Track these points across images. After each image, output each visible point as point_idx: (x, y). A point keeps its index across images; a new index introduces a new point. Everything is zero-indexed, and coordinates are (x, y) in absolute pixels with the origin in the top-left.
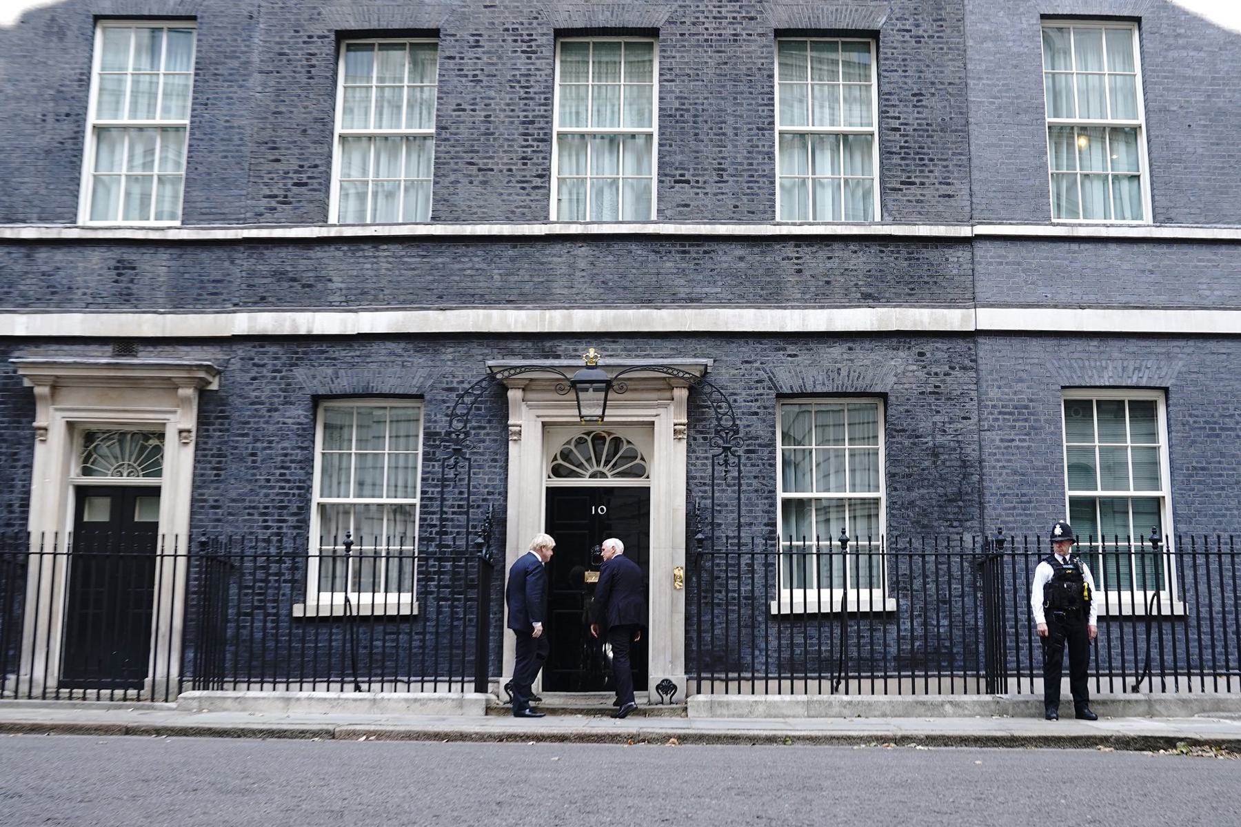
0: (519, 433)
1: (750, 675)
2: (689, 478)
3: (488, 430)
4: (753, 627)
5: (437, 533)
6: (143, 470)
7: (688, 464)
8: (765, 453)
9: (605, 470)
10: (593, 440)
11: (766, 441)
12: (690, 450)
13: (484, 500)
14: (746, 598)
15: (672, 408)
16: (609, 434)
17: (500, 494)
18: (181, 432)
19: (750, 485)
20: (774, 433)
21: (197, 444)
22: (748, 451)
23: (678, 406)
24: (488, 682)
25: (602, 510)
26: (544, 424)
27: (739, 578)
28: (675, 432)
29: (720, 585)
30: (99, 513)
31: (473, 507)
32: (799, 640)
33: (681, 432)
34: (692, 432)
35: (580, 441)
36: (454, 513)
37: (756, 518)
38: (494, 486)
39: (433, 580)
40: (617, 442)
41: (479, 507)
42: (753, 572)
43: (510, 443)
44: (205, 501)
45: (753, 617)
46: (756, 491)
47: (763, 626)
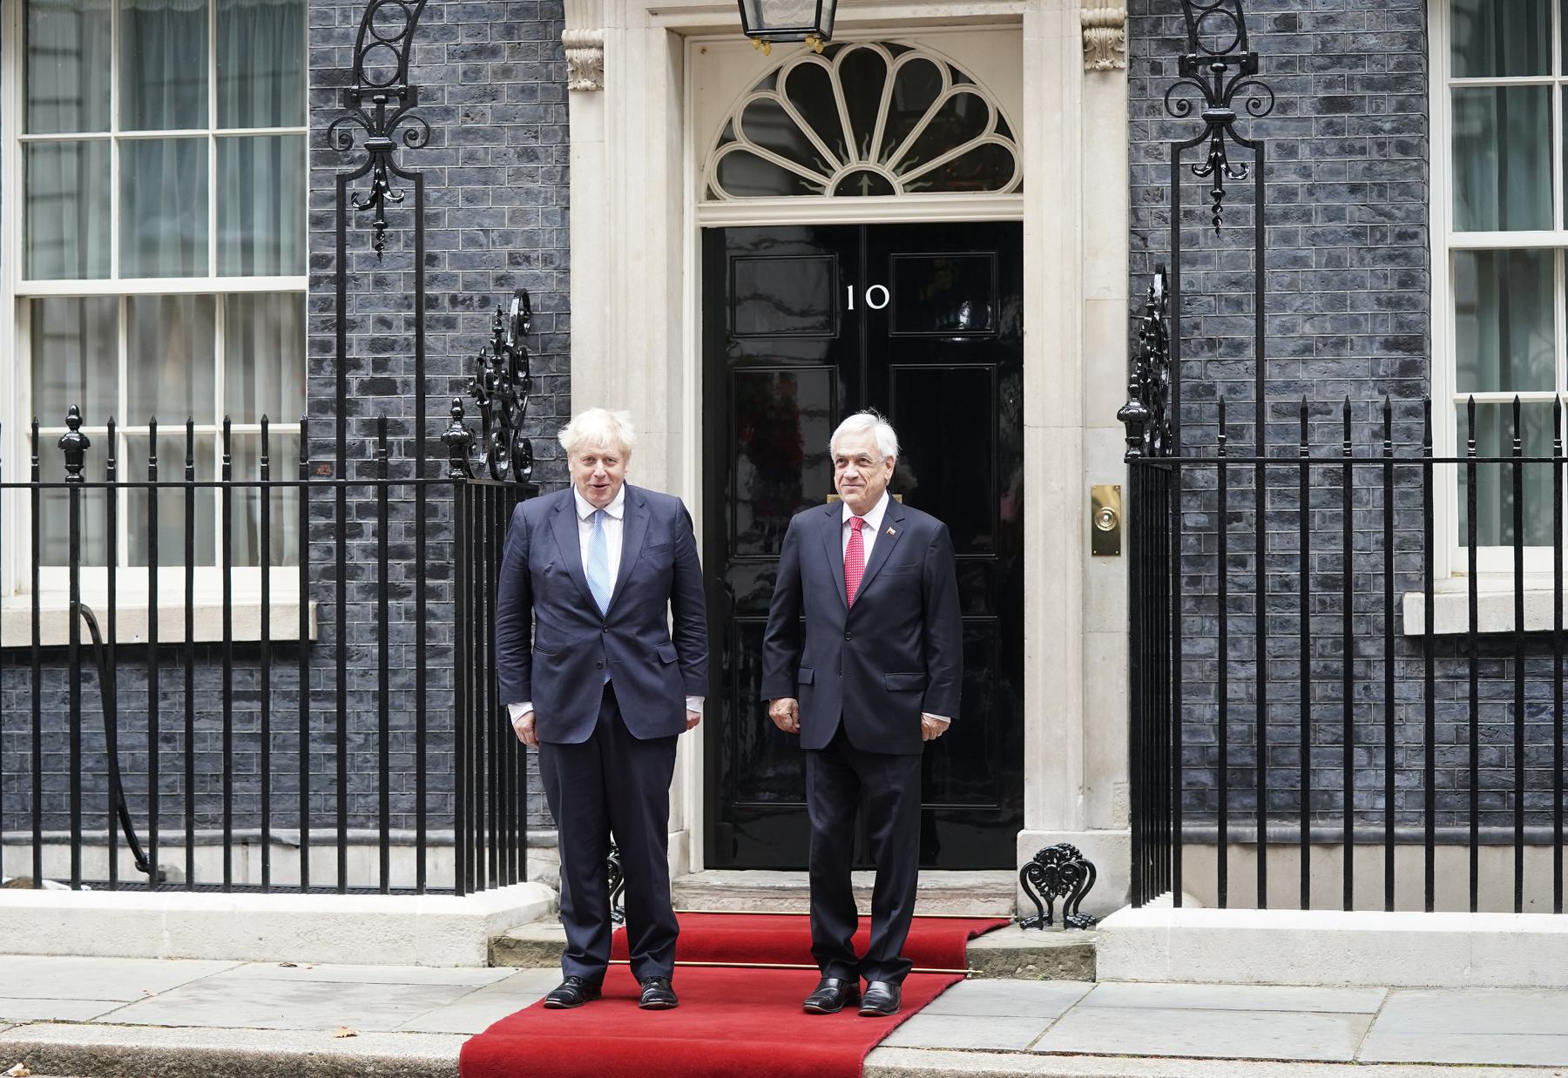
0: (598, 69)
1: (1334, 828)
3: (505, 59)
4: (1348, 678)
5: (366, 388)
7: (1133, 148)
8: (1386, 110)
9: (886, 171)
11: (1390, 69)
13: (501, 281)
14: (1326, 583)
16: (896, 50)
17: (547, 260)
19: (1335, 215)
20: (1418, 42)
22: (1331, 104)
24: (524, 845)
26: (677, 36)
27: (1304, 518)
29: (1242, 539)
31: (466, 303)
32: (1497, 715)
33: (1107, 49)
34: (1148, 47)
35: (806, 84)
37: (1355, 323)
38: (530, 239)
39: (358, 532)
41: (485, 302)
42: (1348, 497)
43: (574, 100)
45: (1348, 643)
46: (1356, 235)
47: (1379, 674)
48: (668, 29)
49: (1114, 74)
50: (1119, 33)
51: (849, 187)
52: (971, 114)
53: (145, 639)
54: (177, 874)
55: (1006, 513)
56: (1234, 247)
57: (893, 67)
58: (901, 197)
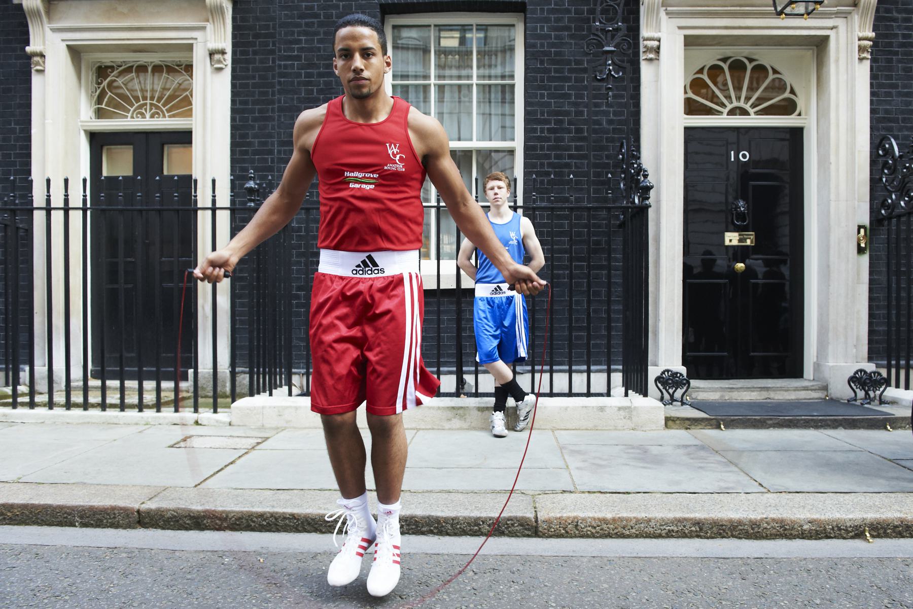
0: (657, 50)
2: (873, 111)
6: (168, 111)
9: (747, 107)
10: (730, 68)
12: (873, 77)
15: (856, 18)
16: (751, 60)
18: (211, 54)
21: (234, 70)
23: (863, 15)
25: (744, 156)
28: (861, 49)
30: (121, 164)
35: (715, 71)
36: (571, 157)
38: (620, 122)
40: (760, 70)
44: (249, 144)
48: (686, 37)
49: (864, 61)
50: (871, 43)
51: (732, 112)
52: (779, 86)
53: (454, 287)
54: (470, 385)
55: (785, 241)
56: (906, 133)
57: (750, 67)
58: (753, 116)
